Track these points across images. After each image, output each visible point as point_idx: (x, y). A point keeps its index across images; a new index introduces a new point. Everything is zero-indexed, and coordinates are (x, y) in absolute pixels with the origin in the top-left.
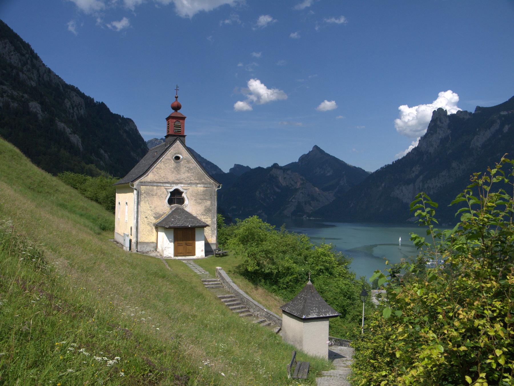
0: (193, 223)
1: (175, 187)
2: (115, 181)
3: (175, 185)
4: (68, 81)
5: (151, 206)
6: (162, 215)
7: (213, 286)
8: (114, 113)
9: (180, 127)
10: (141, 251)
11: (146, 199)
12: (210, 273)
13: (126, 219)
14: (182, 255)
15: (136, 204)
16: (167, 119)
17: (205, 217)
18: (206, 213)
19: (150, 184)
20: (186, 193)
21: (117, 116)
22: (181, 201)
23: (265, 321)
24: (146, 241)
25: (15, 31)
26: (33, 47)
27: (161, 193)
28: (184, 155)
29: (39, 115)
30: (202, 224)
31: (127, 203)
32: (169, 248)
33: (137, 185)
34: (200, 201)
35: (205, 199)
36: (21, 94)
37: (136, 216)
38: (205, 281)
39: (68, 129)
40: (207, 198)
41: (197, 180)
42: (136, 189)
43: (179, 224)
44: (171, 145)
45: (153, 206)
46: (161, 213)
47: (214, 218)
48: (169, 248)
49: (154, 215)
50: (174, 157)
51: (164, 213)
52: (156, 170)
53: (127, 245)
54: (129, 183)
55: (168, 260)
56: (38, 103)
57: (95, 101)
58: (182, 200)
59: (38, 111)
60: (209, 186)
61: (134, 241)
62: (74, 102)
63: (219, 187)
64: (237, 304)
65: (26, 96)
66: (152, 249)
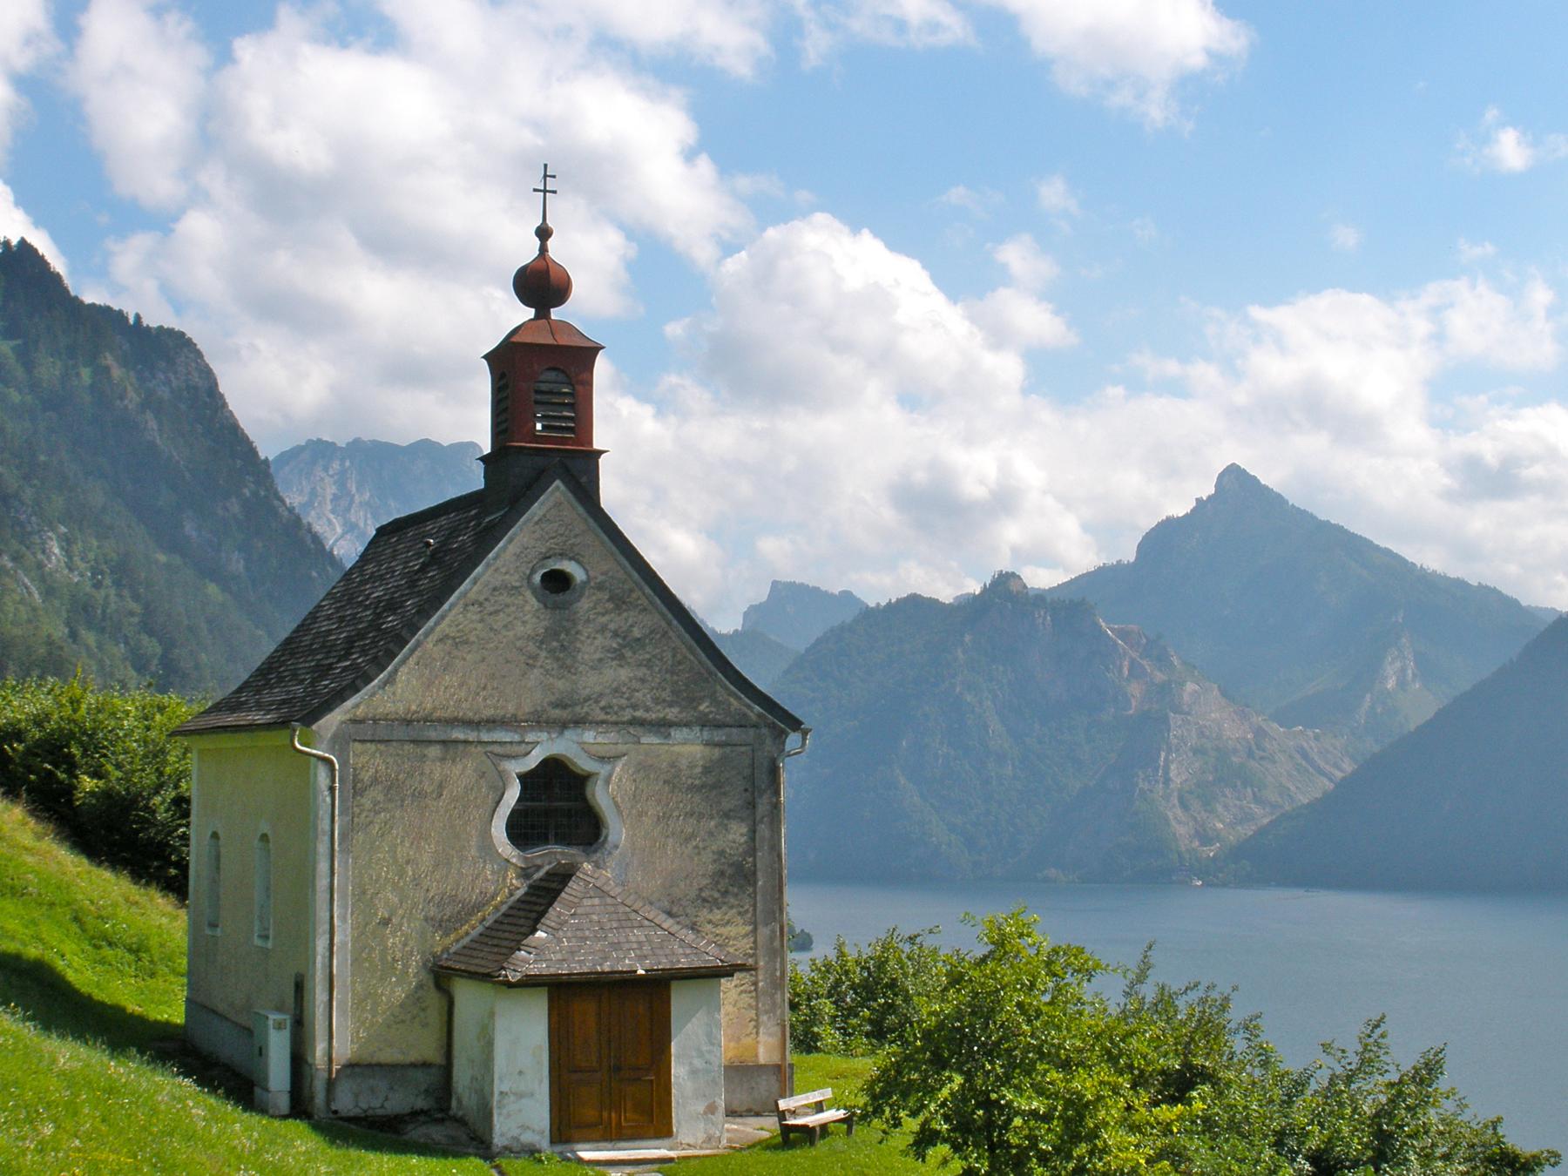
3: (544, 736)
6: (478, 907)
32: (520, 1096)
48: (520, 1096)
50: (537, 578)
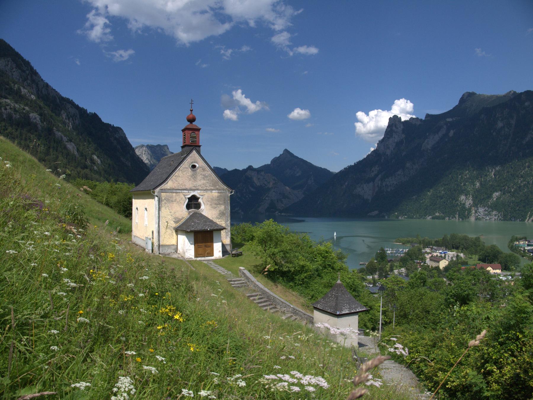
0: (211, 226)
1: (192, 193)
2: (133, 188)
3: (192, 192)
4: (64, 95)
5: (171, 211)
6: (182, 219)
7: (239, 285)
8: (105, 122)
9: (196, 138)
10: (163, 253)
11: (166, 205)
12: (232, 272)
13: (146, 223)
14: (202, 256)
15: (157, 210)
16: (183, 131)
17: (219, 220)
18: (221, 217)
19: (169, 191)
20: (202, 199)
21: (108, 126)
22: (198, 206)
23: (291, 316)
24: (167, 244)
25: (17, 50)
26: (33, 64)
27: (180, 199)
28: (200, 163)
29: (39, 126)
30: (220, 227)
31: (146, 209)
32: (190, 250)
33: (158, 192)
34: (215, 206)
35: (220, 204)
36: (22, 107)
37: (157, 221)
38: (231, 281)
39: (65, 137)
40: (221, 203)
41: (212, 186)
42: (157, 196)
43: (199, 228)
44: (188, 155)
45: (173, 212)
46: (181, 217)
47: (228, 221)
48: (190, 250)
49: (174, 220)
50: (191, 166)
51: (183, 218)
52: (175, 178)
53: (150, 247)
54: (150, 190)
55: (190, 261)
56: (38, 115)
57: (88, 112)
58: (198, 205)
59: (38, 122)
60: (222, 191)
61: (156, 244)
62: (69, 113)
63: (231, 192)
64: (265, 302)
65: (27, 108)
66: (173, 251)
